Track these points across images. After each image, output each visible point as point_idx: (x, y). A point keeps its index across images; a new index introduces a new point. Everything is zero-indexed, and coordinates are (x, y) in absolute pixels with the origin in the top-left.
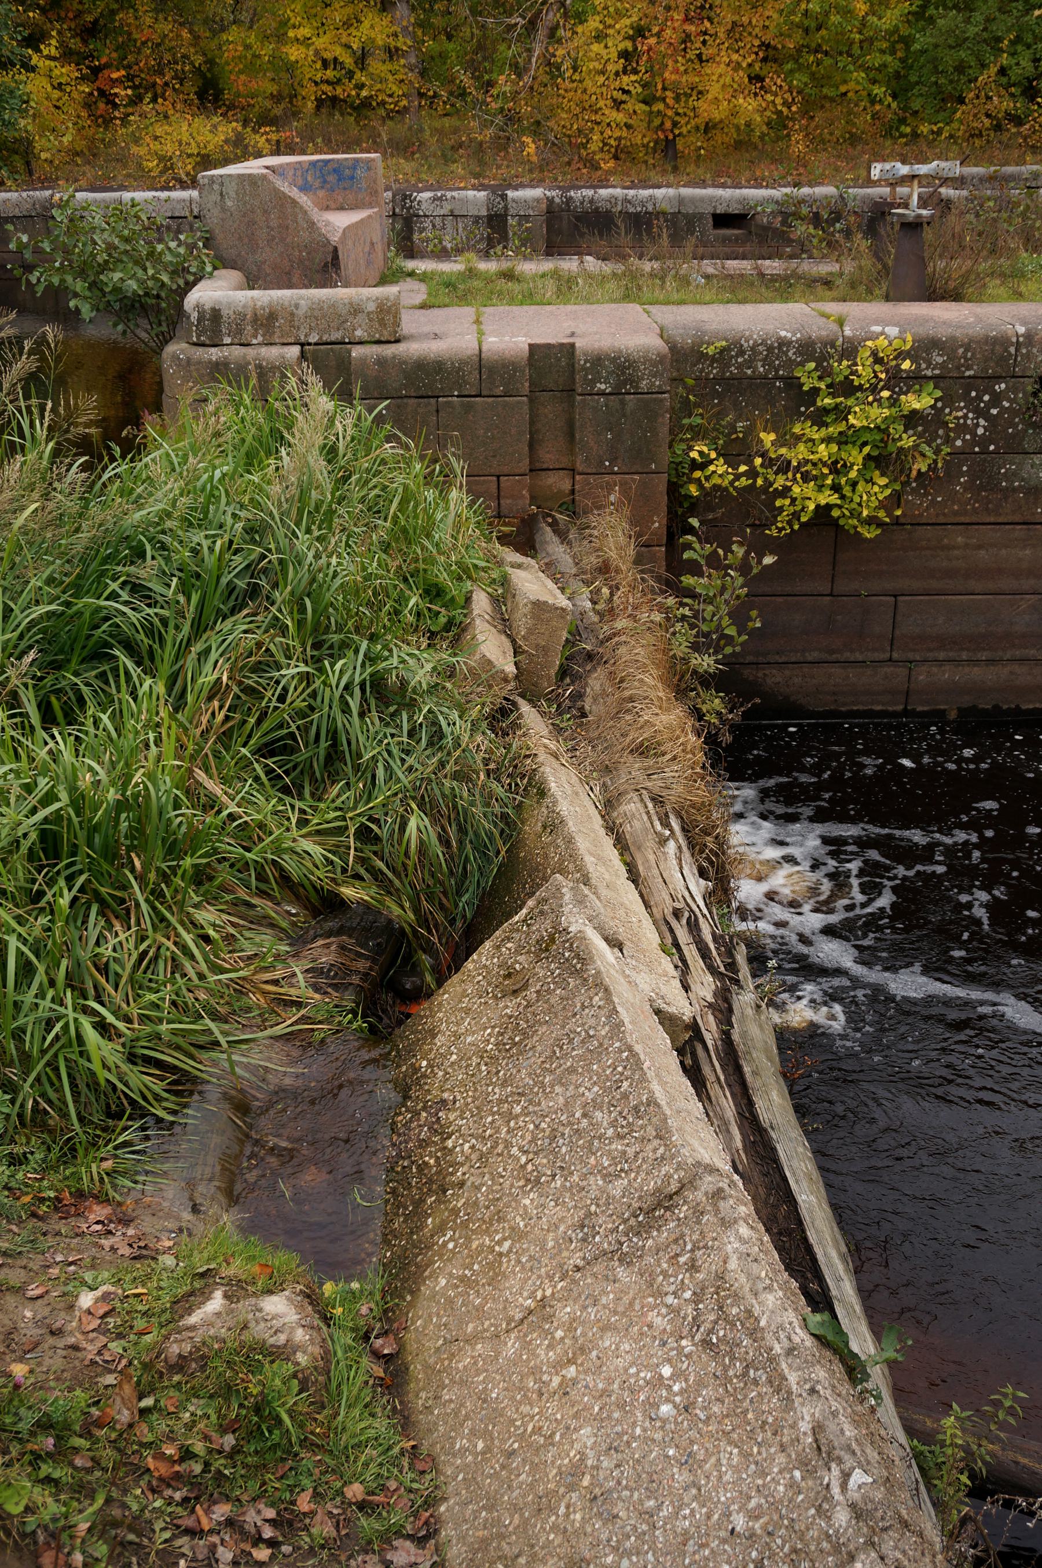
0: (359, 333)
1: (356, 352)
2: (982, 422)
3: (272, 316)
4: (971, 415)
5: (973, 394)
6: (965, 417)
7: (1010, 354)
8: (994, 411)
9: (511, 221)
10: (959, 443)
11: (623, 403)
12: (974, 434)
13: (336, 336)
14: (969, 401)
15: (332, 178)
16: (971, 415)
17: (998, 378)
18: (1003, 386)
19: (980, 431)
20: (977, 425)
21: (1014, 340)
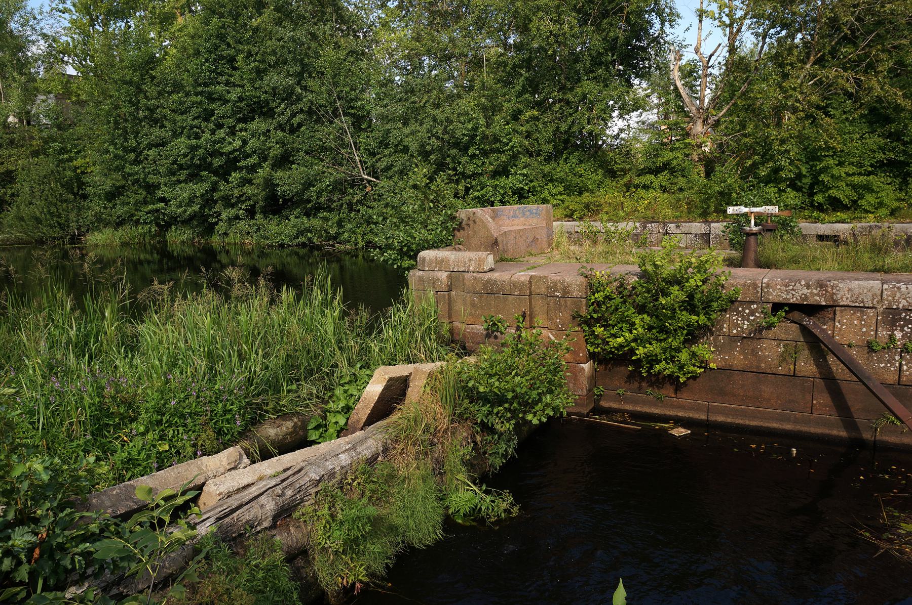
0: (471, 268)
1: (466, 275)
2: (746, 322)
3: (442, 261)
4: (740, 319)
5: (740, 309)
6: (737, 319)
7: (758, 292)
8: (752, 318)
9: (712, 236)
10: (735, 331)
11: (566, 302)
12: (742, 328)
13: (462, 269)
14: (739, 313)
15: (528, 213)
16: (740, 319)
17: (753, 303)
18: (755, 306)
19: (745, 327)
20: (744, 324)
21: (760, 285)
